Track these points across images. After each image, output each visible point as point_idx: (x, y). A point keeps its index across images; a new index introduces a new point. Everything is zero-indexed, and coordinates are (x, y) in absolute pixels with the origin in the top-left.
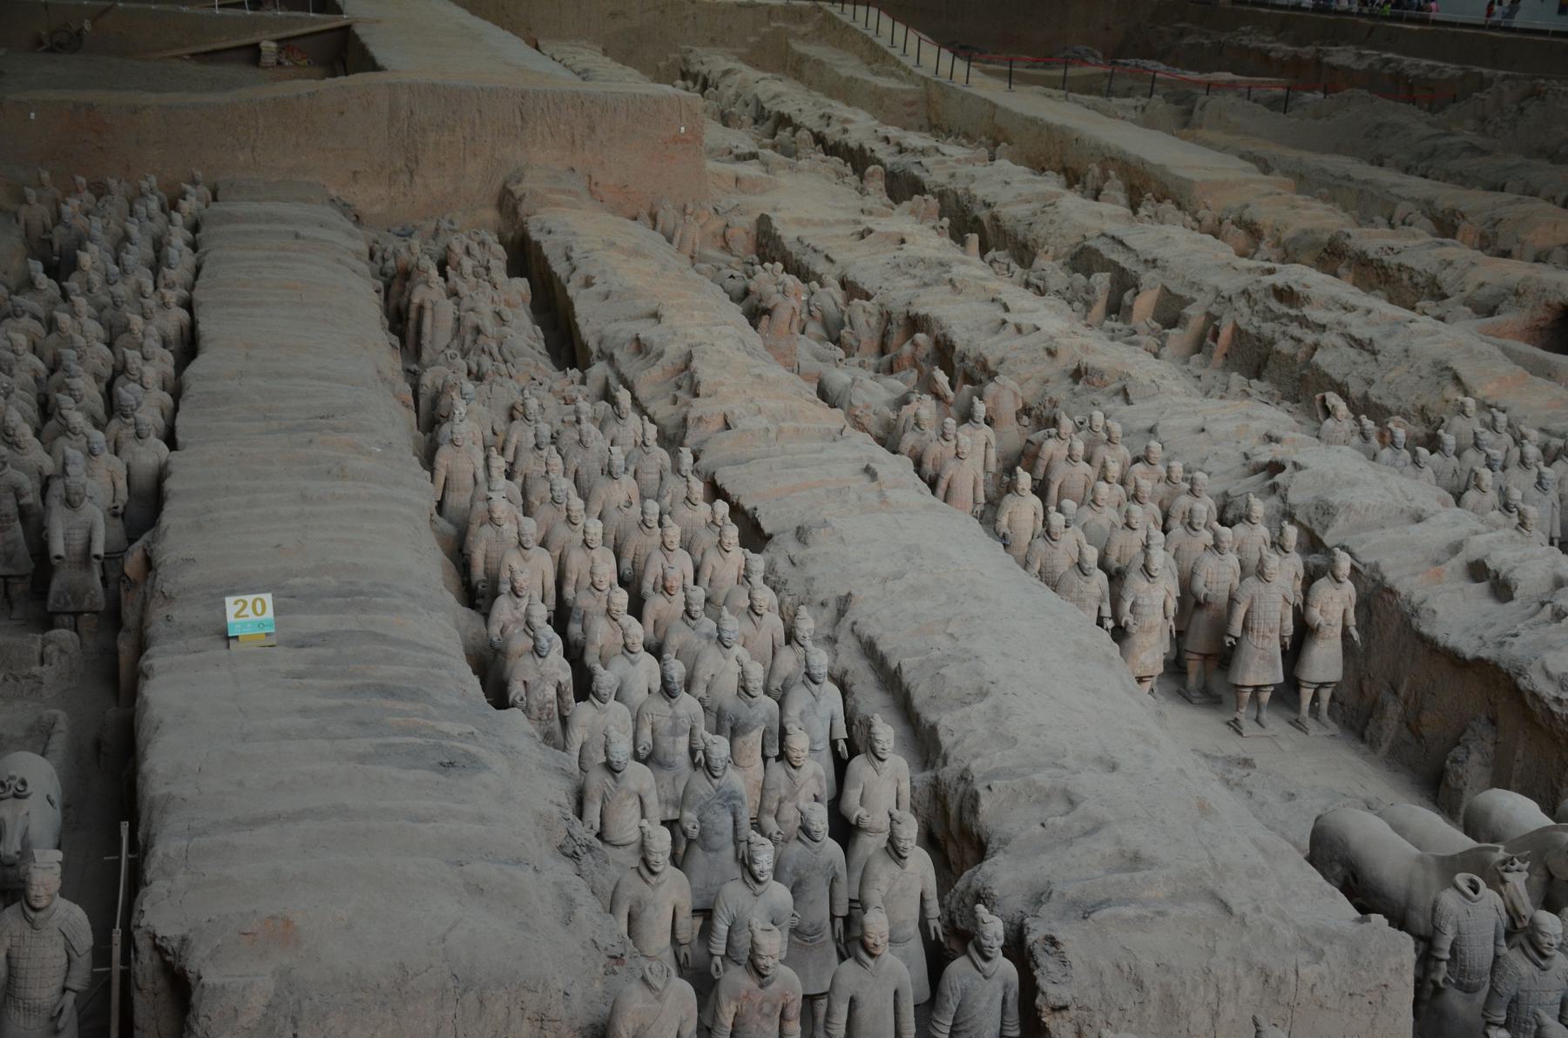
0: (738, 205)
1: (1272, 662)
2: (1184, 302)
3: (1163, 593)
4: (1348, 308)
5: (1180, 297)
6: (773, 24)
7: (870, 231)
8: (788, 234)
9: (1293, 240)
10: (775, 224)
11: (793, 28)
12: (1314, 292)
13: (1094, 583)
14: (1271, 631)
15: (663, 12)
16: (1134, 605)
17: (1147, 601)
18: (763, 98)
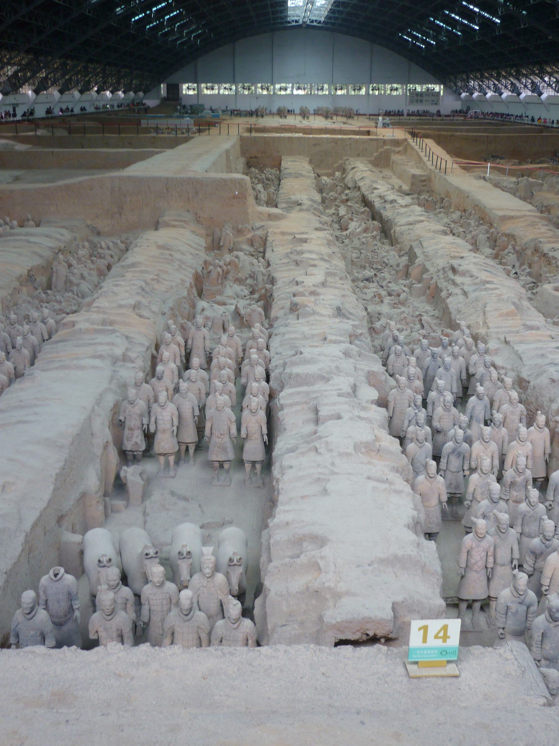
0: (263, 226)
1: (224, 450)
2: (427, 270)
3: (169, 414)
4: (472, 276)
5: (427, 269)
6: (386, 147)
7: (295, 237)
8: (270, 239)
9: (525, 244)
10: (269, 234)
11: (393, 148)
12: (461, 269)
13: (136, 407)
14: (221, 435)
15: (336, 143)
16: (156, 419)
17: (161, 418)
18: (357, 179)
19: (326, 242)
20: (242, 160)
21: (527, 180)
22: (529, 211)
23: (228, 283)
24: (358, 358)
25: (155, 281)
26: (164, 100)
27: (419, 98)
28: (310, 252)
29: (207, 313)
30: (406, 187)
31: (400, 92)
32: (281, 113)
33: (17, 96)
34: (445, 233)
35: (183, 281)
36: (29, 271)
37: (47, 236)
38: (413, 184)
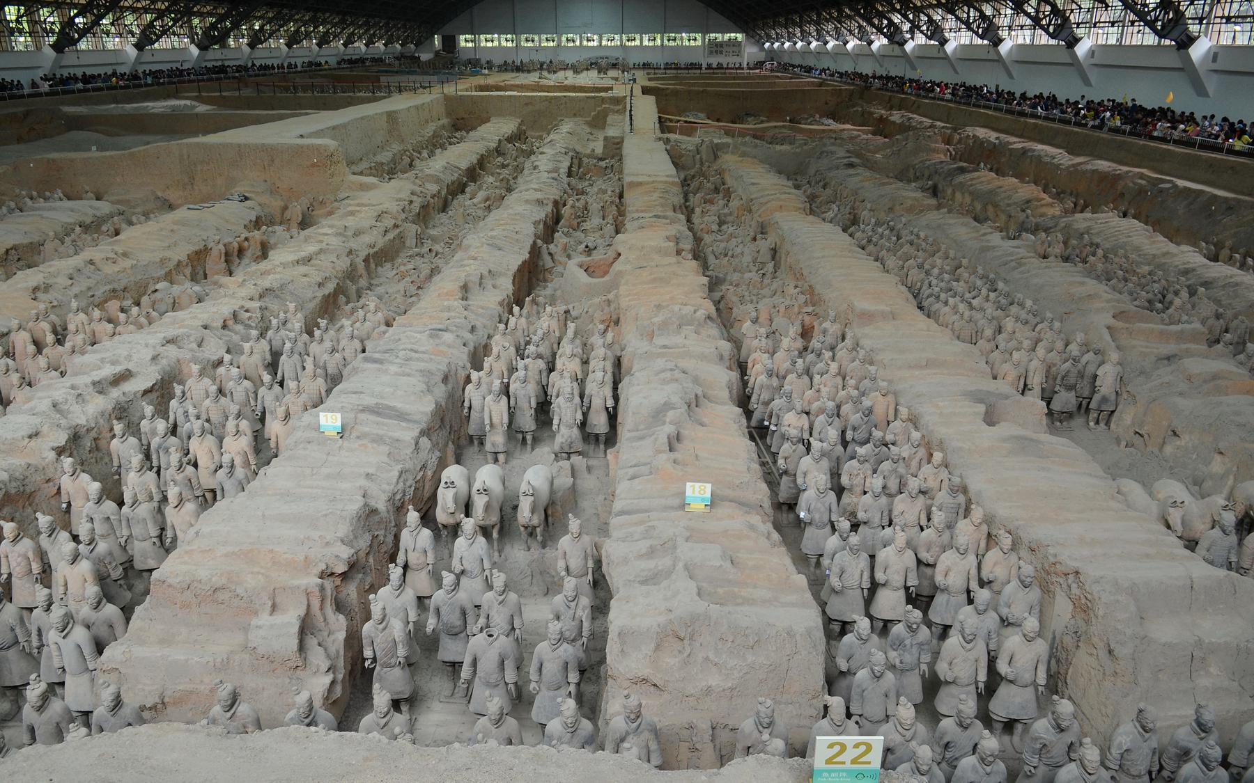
19: (376, 214)
20: (445, 121)
21: (712, 142)
22: (667, 176)
23: (246, 261)
24: (194, 346)
25: (110, 261)
26: (437, 53)
27: (719, 49)
28: (331, 227)
29: (156, 294)
30: (599, 150)
31: (699, 43)
32: (552, 67)
33: (225, 51)
34: (540, 203)
35: (162, 261)
36: (7, 251)
37: (72, 211)
38: (605, 147)
